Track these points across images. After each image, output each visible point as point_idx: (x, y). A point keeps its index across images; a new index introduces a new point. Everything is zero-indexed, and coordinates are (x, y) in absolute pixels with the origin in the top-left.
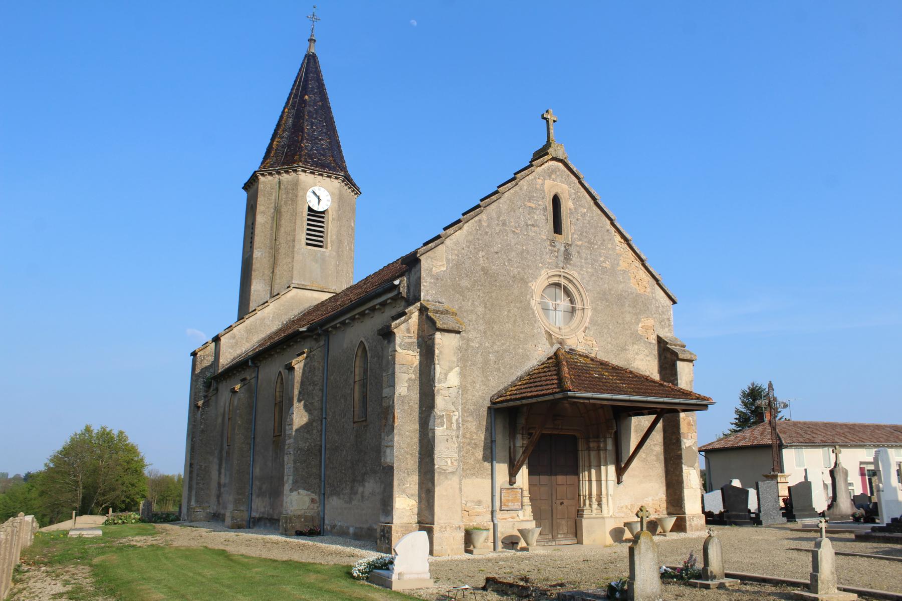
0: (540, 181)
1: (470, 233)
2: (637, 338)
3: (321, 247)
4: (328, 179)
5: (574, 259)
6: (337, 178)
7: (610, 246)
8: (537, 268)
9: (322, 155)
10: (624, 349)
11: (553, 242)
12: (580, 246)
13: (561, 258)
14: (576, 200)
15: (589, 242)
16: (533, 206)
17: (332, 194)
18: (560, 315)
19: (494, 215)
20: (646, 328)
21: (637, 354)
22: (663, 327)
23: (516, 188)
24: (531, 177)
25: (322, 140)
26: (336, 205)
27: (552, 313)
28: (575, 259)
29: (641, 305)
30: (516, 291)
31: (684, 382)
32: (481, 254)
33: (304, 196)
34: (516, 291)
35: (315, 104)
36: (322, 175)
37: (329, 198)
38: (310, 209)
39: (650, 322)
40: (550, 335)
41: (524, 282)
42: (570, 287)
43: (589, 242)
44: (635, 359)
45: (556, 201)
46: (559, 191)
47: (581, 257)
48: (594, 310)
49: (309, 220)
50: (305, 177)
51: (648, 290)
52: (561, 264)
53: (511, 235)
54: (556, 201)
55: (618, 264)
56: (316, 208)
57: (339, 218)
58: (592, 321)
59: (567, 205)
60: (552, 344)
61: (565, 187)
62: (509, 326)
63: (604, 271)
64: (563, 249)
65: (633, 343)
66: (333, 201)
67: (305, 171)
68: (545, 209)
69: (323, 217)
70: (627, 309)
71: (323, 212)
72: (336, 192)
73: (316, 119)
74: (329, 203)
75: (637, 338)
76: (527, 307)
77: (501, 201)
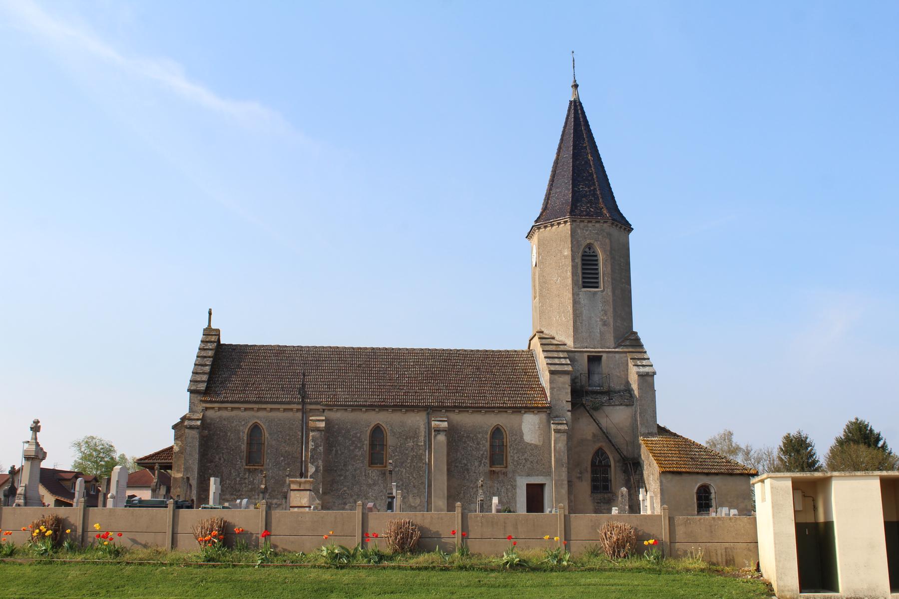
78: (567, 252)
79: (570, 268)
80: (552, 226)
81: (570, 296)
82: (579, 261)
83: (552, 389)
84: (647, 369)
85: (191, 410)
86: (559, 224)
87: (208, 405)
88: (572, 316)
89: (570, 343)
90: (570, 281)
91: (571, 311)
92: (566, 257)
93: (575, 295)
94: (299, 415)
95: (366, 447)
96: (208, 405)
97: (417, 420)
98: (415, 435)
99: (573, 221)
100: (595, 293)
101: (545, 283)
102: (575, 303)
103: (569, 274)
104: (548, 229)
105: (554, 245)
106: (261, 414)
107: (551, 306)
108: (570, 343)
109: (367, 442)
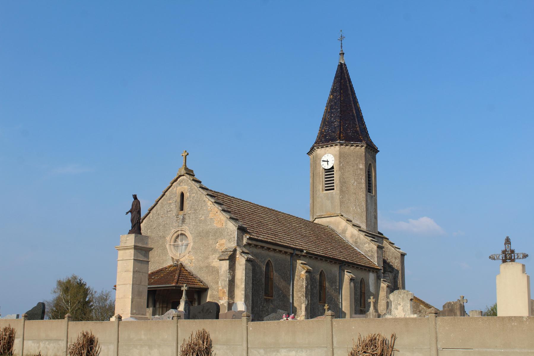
0: (175, 189)
1: (145, 223)
2: (215, 251)
3: (333, 189)
4: (332, 147)
5: (186, 221)
6: (336, 145)
7: (205, 208)
8: (170, 230)
9: (334, 132)
10: (207, 258)
11: (177, 216)
12: (190, 214)
13: (181, 222)
14: (191, 191)
15: (195, 210)
16: (171, 202)
17: (335, 156)
18: (184, 247)
19: (155, 212)
20: (221, 245)
21: (214, 259)
22: (230, 242)
23: (164, 197)
24: (171, 189)
25: (335, 122)
26: (338, 162)
27: (180, 248)
28: (187, 221)
29: (218, 233)
30: (161, 243)
31: (222, 271)
32: (149, 230)
33: (320, 163)
34: (161, 243)
35: (335, 99)
36: (327, 147)
37: (333, 159)
38: (325, 170)
39: (224, 241)
40: (173, 258)
41: (164, 237)
42: (186, 234)
43: (195, 210)
44: (213, 262)
45: (182, 195)
46: (182, 190)
47: (190, 219)
48: (194, 242)
49: (326, 175)
50: (319, 151)
51: (224, 224)
52: (180, 225)
53: (161, 219)
54: (182, 195)
55: (208, 216)
56: (326, 168)
57: (341, 168)
58: (193, 248)
59: (186, 195)
60: (173, 262)
61: (186, 187)
62: (157, 258)
63: (201, 221)
64: (182, 217)
65: (213, 254)
66: (335, 160)
67: (318, 148)
68: (176, 202)
69: (333, 171)
70: (211, 237)
71: (333, 168)
72: (338, 153)
73: (335, 108)
74: (333, 162)
75: (215, 251)
76: (165, 248)
77: (158, 205)
78: (362, 166)
79: (364, 177)
80: (352, 146)
81: (364, 196)
82: (367, 173)
83: (378, 257)
84: (401, 251)
85: (238, 245)
86: (357, 146)
87: (250, 242)
88: (365, 209)
89: (364, 227)
90: (364, 186)
91: (365, 206)
92: (361, 169)
93: (366, 195)
94: (288, 258)
95: (318, 287)
96: (250, 242)
97: (335, 269)
98: (335, 282)
99: (366, 147)
100: (372, 197)
101: (345, 182)
102: (367, 201)
103: (363, 181)
104: (347, 147)
105: (352, 159)
106: (272, 254)
107: (349, 200)
108: (364, 227)
109: (318, 284)
